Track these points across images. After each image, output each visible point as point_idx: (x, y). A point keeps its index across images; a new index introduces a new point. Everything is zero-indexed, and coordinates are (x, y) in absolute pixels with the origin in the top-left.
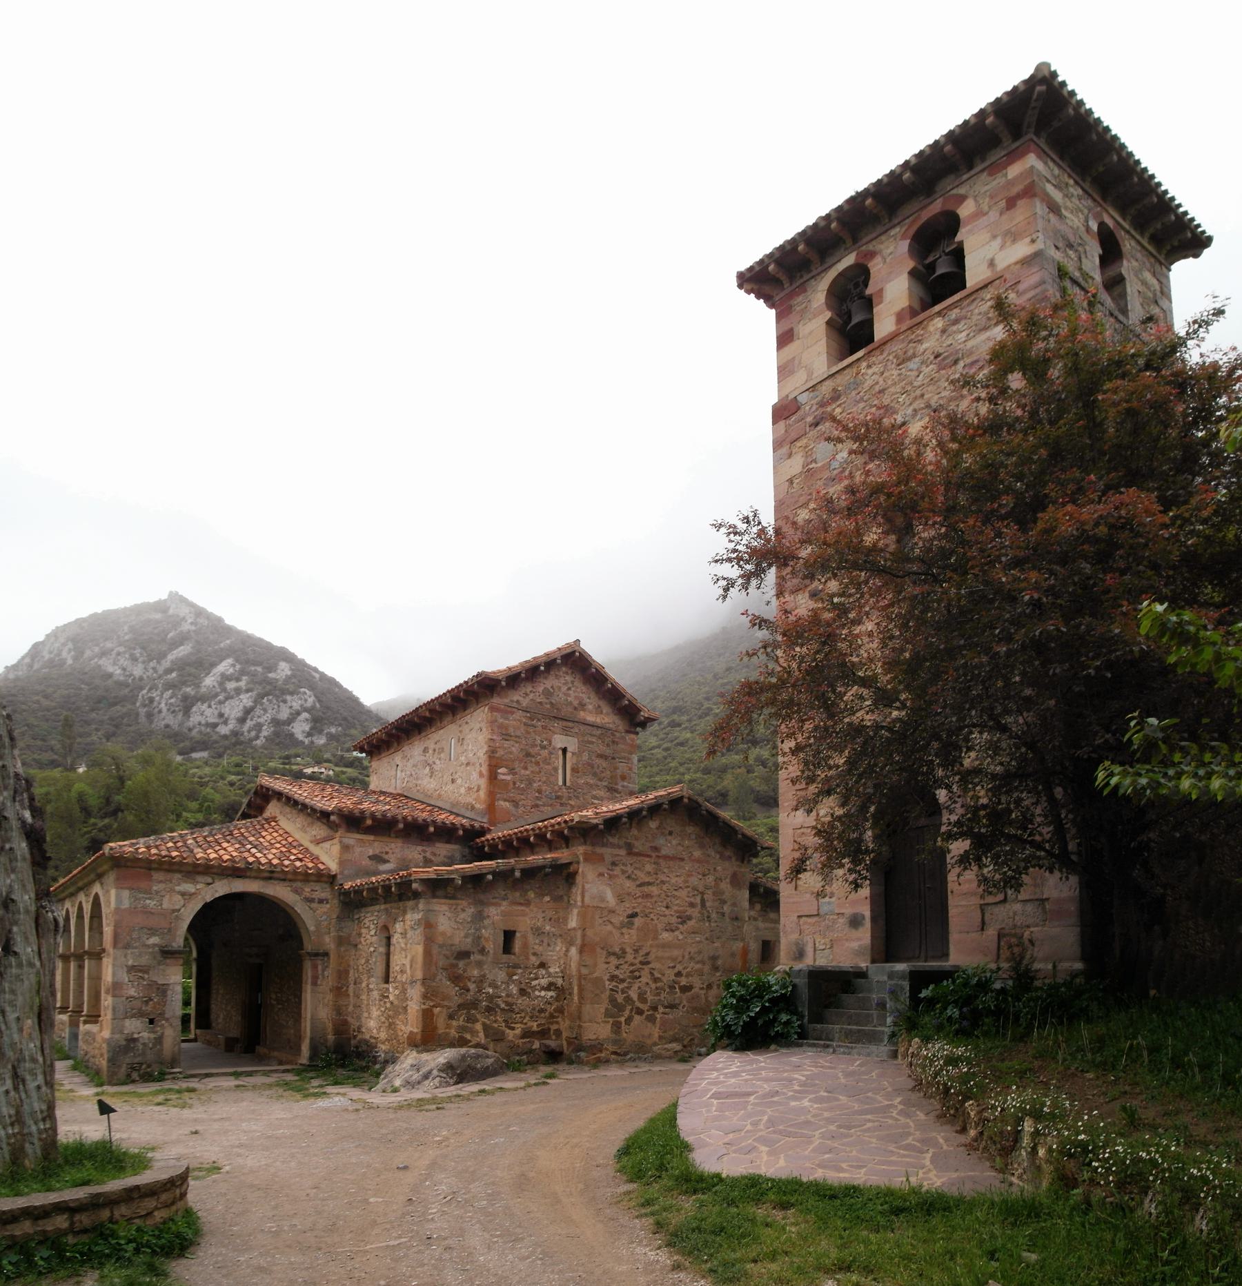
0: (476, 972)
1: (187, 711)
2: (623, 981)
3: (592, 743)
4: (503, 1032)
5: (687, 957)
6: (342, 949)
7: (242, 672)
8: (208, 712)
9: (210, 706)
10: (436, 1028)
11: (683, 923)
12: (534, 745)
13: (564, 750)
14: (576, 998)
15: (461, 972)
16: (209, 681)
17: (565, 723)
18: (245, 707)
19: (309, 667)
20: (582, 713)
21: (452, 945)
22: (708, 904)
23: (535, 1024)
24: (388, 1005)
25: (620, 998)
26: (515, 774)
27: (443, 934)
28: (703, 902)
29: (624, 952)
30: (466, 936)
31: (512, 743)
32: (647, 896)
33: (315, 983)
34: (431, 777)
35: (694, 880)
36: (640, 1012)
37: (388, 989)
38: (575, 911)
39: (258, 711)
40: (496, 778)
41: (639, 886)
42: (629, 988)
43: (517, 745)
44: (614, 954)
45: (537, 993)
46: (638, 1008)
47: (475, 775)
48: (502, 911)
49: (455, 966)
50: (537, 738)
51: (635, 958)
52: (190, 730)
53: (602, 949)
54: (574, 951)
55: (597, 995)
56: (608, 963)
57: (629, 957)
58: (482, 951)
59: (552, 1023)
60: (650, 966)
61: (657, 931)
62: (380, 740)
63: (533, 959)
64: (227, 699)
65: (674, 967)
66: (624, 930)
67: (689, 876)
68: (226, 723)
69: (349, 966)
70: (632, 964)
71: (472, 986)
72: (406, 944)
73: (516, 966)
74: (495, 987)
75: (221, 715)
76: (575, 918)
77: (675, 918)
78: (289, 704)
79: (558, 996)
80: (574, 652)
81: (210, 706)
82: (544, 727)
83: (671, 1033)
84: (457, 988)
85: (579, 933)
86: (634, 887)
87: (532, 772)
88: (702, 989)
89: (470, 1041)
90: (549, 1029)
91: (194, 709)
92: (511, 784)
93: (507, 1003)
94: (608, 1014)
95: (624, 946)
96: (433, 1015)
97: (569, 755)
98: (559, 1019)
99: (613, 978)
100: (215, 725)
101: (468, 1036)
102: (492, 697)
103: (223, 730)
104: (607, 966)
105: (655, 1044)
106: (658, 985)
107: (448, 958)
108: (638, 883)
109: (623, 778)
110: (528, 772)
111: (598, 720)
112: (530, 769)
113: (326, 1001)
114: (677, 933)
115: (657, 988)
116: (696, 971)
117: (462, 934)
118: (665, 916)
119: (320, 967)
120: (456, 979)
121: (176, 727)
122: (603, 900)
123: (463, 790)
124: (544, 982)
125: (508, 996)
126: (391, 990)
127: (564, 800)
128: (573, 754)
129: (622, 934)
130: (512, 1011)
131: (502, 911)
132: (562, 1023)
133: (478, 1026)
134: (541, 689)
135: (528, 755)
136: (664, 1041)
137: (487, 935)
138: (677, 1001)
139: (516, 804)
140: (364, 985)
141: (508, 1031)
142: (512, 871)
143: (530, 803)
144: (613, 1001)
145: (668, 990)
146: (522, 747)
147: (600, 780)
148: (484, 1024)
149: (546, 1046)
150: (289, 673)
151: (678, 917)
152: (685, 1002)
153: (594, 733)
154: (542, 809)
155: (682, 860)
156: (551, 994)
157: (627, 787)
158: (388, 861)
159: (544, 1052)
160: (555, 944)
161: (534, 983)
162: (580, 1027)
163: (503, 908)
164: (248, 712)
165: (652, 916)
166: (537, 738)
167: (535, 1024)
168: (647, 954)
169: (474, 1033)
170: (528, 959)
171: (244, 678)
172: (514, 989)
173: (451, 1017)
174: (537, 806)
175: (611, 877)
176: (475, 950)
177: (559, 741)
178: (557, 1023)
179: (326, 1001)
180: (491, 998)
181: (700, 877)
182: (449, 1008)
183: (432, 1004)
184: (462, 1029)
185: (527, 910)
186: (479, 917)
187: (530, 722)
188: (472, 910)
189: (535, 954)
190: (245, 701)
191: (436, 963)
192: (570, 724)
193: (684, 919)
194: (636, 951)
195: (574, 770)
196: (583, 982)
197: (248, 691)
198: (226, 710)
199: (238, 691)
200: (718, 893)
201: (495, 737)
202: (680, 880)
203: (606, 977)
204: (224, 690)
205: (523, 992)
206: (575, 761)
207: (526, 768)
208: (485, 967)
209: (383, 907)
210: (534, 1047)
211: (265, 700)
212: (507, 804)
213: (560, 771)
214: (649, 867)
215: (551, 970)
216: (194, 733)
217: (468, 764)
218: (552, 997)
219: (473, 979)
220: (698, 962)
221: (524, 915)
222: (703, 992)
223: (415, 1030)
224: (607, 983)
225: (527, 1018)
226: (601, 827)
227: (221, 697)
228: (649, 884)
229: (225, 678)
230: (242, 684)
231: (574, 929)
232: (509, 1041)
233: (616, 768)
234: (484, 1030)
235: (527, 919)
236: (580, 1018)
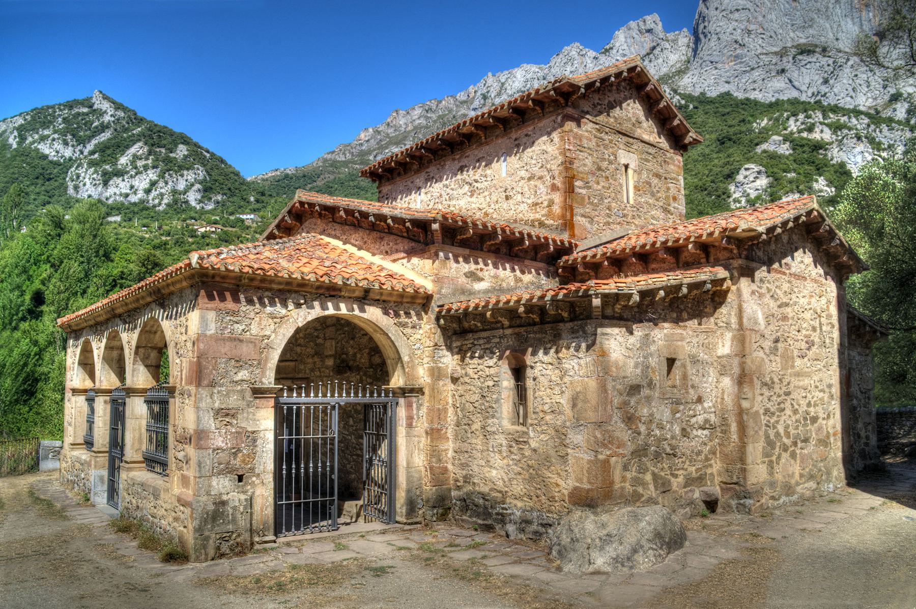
0: (645, 411)
1: (106, 184)
2: (773, 414)
3: (647, 160)
4: (669, 481)
6: (441, 383)
7: (150, 153)
8: (122, 185)
9: (123, 180)
10: (612, 483)
12: (604, 160)
13: (627, 167)
14: (735, 437)
15: (632, 411)
16: (123, 160)
17: (625, 139)
18: (150, 180)
19: (202, 148)
20: (639, 131)
21: (624, 377)
22: (824, 328)
23: (694, 468)
24: (527, 453)
25: (772, 433)
26: (589, 188)
27: (616, 363)
28: (820, 324)
29: (773, 383)
30: (636, 366)
31: (586, 155)
32: (785, 318)
33: (410, 426)
34: (472, 196)
36: (785, 448)
37: (527, 433)
38: (729, 335)
39: (161, 184)
40: (573, 192)
41: (779, 307)
42: (777, 422)
43: (590, 158)
44: (766, 384)
45: (695, 432)
46: (784, 444)
47: (543, 189)
48: (665, 335)
49: (626, 403)
50: (606, 152)
51: (780, 388)
52: (107, 199)
53: (758, 378)
54: (727, 382)
55: (756, 432)
56: (762, 395)
57: (777, 386)
58: (650, 384)
59: (706, 467)
60: (792, 396)
61: (793, 358)
62: (398, 163)
63: (691, 391)
64: (136, 174)
65: (806, 397)
66: (772, 357)
68: (135, 193)
69: (447, 403)
70: (779, 396)
71: (643, 428)
72: (561, 379)
73: (678, 403)
74: (662, 428)
75: (132, 187)
76: (728, 344)
77: (803, 343)
78: (185, 177)
79: (711, 434)
80: (636, 67)
82: (611, 141)
83: (807, 470)
84: (629, 432)
85: (736, 362)
86: (776, 308)
87: (603, 187)
88: (824, 419)
89: (643, 496)
90: (706, 473)
91: (111, 182)
92: (587, 198)
93: (673, 448)
94: (766, 455)
95: (773, 376)
96: (610, 465)
97: (630, 172)
98: (713, 461)
99: (767, 411)
100: (127, 195)
101: (640, 490)
102: (567, 105)
103: (134, 199)
104: (760, 398)
105: (798, 484)
106: (798, 416)
107: (621, 394)
108: (779, 303)
109: (675, 199)
110: (599, 187)
111: (651, 139)
112: (602, 184)
113: (421, 445)
114: (806, 359)
115: (796, 421)
116: (820, 399)
117: (632, 364)
118: (797, 341)
119: (414, 405)
120: (630, 419)
122: (756, 323)
123: (523, 207)
124: (700, 419)
125: (673, 438)
126: (532, 434)
127: (629, 219)
128: (635, 171)
129: (771, 361)
130: (675, 456)
131: (665, 335)
132: (714, 465)
133: (648, 477)
134: (606, 102)
135: (599, 169)
136: (803, 480)
137: (653, 364)
138: (809, 435)
139: (591, 220)
140: (476, 426)
141: (673, 479)
142: (679, 287)
143: (602, 220)
144: (767, 437)
145: (803, 422)
146: (594, 159)
147: (657, 200)
148: (654, 474)
149: (706, 494)
150: (186, 153)
151: (807, 342)
152: (814, 435)
153: (650, 151)
154: (612, 227)
156: (706, 432)
157: (677, 209)
158: (482, 279)
159: (705, 502)
160: (709, 374)
161: (694, 420)
162: (744, 470)
163: (665, 331)
164: (153, 184)
165: (789, 339)
166: (606, 152)
167: (694, 468)
168: (789, 384)
169: (644, 484)
170: (687, 393)
171: (151, 157)
172: (677, 429)
173: (625, 468)
174: (608, 223)
175: (761, 296)
176: (644, 383)
177: (624, 157)
178: (711, 465)
179: (421, 445)
180: (660, 440)
181: (817, 298)
182: (624, 456)
183: (608, 453)
184: (637, 481)
185: (684, 333)
186: (646, 340)
187: (599, 135)
188: (640, 333)
189: (693, 387)
190: (151, 175)
191: (611, 402)
192: (631, 140)
194: (780, 380)
195: (635, 187)
196: (745, 417)
197: (154, 167)
198: (136, 182)
201: (571, 148)
203: (762, 411)
204: (136, 168)
205: (685, 433)
206: (636, 179)
207: (598, 183)
208: (653, 404)
209: (508, 332)
210: (695, 497)
211: (166, 175)
212: (584, 219)
213: (624, 188)
214: (786, 287)
215: (706, 405)
217: (529, 179)
218: (706, 435)
219: (643, 419)
220: (821, 391)
221: (682, 339)
222: (824, 422)
223: (587, 486)
224: (762, 417)
225: (688, 463)
226: (764, 237)
228: (787, 305)
229: (136, 157)
230: (150, 162)
231: (728, 356)
232: (674, 492)
233: (668, 189)
234: (654, 480)
235: (684, 343)
236: (742, 459)
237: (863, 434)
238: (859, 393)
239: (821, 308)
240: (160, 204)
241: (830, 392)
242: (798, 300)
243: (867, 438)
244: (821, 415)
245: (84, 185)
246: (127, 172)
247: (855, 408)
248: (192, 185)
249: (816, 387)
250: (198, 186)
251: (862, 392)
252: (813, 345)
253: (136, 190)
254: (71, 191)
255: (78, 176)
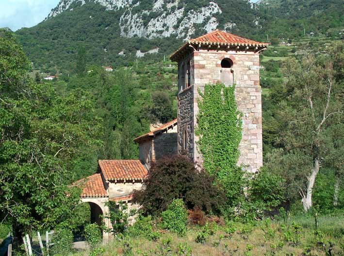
1: (145, 25)
8: (158, 24)
9: (158, 21)
18: (178, 19)
39: (186, 20)
52: (148, 36)
64: (167, 15)
68: (167, 30)
75: (164, 25)
78: (203, 13)
81: (158, 21)
91: (150, 24)
100: (161, 32)
103: (167, 34)
121: (140, 36)
164: (179, 21)
197: (179, 8)
199: (173, 9)
204: (166, 10)
216: (150, 38)
227: (164, 14)
240: (185, 36)
245: (131, 28)
246: (160, 15)
248: (209, 18)
250: (214, 19)
253: (168, 27)
254: (123, 34)
255: (126, 21)
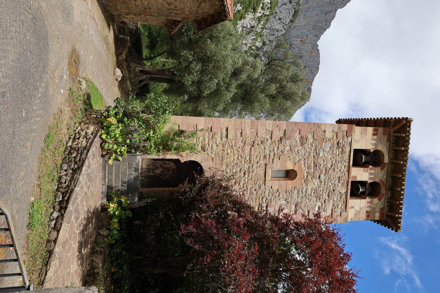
5: (151, 2)
11: (167, 3)
22: (176, 11)
28: (177, 10)
35: (187, 9)
67: (190, 8)
151: (170, 3)
155: (198, 7)
181: (189, 11)
193: (169, 4)
200: (180, 14)
202: (189, 6)
220: (148, 4)
222: (134, 4)
237: (128, 16)
238: (146, 18)
239: (184, 11)
241: (147, 8)
242: (189, 3)
243: (127, 18)
244: (137, 3)
247: (140, 15)
249: (150, 3)
251: (147, 19)
252: (169, 5)
